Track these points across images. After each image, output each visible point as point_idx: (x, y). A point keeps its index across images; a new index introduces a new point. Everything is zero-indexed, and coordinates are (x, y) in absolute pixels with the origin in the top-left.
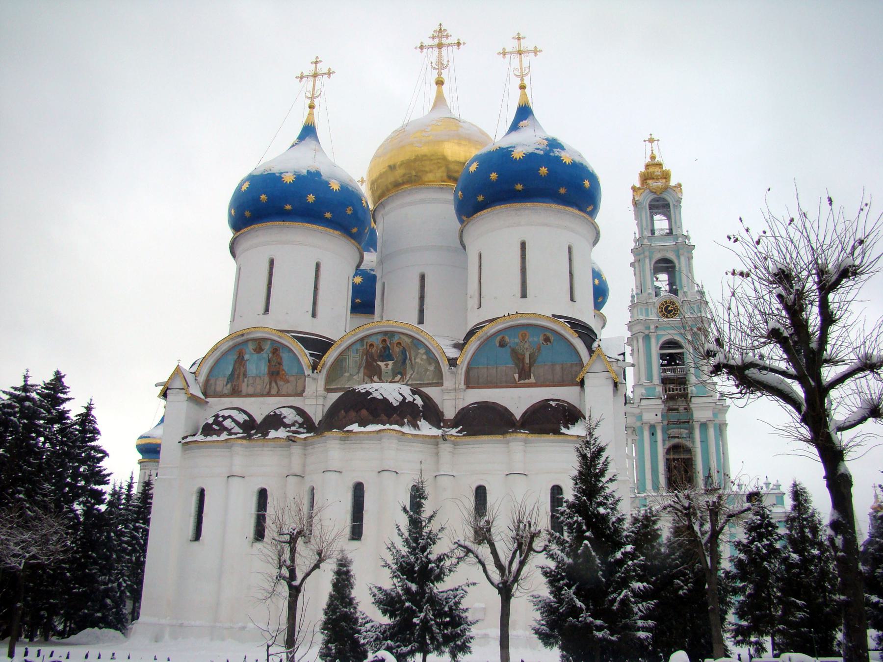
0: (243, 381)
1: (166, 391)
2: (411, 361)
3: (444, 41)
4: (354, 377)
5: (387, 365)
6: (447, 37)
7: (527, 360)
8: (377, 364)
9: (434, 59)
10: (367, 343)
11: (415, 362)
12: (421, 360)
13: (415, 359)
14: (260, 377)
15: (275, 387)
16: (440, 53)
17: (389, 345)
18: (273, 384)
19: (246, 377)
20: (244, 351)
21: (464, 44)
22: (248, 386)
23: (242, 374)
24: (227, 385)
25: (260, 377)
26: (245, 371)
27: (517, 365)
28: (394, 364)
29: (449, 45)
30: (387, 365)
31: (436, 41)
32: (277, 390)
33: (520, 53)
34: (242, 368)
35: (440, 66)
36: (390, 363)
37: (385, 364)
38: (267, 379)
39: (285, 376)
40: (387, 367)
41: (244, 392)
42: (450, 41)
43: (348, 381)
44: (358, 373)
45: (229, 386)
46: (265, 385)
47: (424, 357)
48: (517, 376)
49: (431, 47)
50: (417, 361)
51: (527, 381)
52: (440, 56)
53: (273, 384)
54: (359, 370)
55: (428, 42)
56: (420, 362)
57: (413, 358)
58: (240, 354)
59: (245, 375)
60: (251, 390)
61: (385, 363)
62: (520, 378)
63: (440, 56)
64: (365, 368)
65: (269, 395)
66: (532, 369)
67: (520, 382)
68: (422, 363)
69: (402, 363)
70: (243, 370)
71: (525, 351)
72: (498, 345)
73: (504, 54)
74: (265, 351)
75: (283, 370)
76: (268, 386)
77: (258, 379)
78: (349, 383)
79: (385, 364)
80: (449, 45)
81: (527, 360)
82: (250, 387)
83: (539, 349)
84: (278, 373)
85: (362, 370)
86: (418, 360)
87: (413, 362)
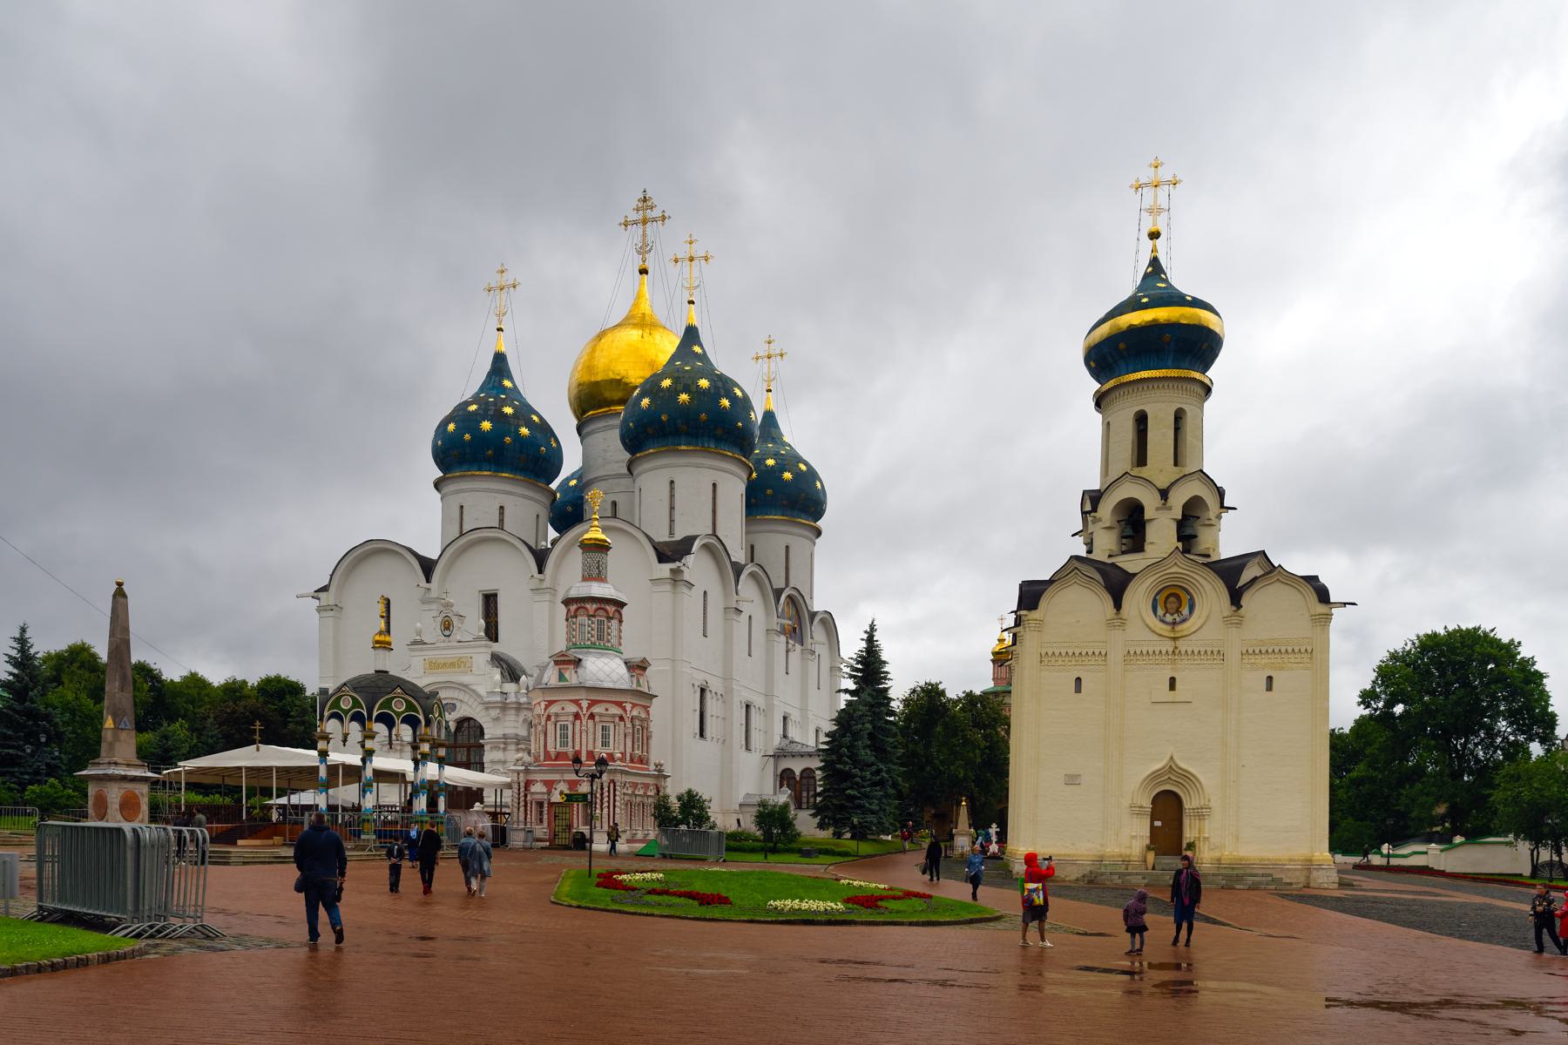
3: (650, 214)
6: (652, 208)
9: (638, 240)
16: (644, 231)
21: (670, 217)
29: (654, 220)
31: (639, 216)
33: (691, 259)
35: (644, 250)
42: (656, 213)
49: (635, 223)
52: (644, 235)
55: (633, 216)
63: (644, 235)
73: (676, 261)
80: (654, 220)
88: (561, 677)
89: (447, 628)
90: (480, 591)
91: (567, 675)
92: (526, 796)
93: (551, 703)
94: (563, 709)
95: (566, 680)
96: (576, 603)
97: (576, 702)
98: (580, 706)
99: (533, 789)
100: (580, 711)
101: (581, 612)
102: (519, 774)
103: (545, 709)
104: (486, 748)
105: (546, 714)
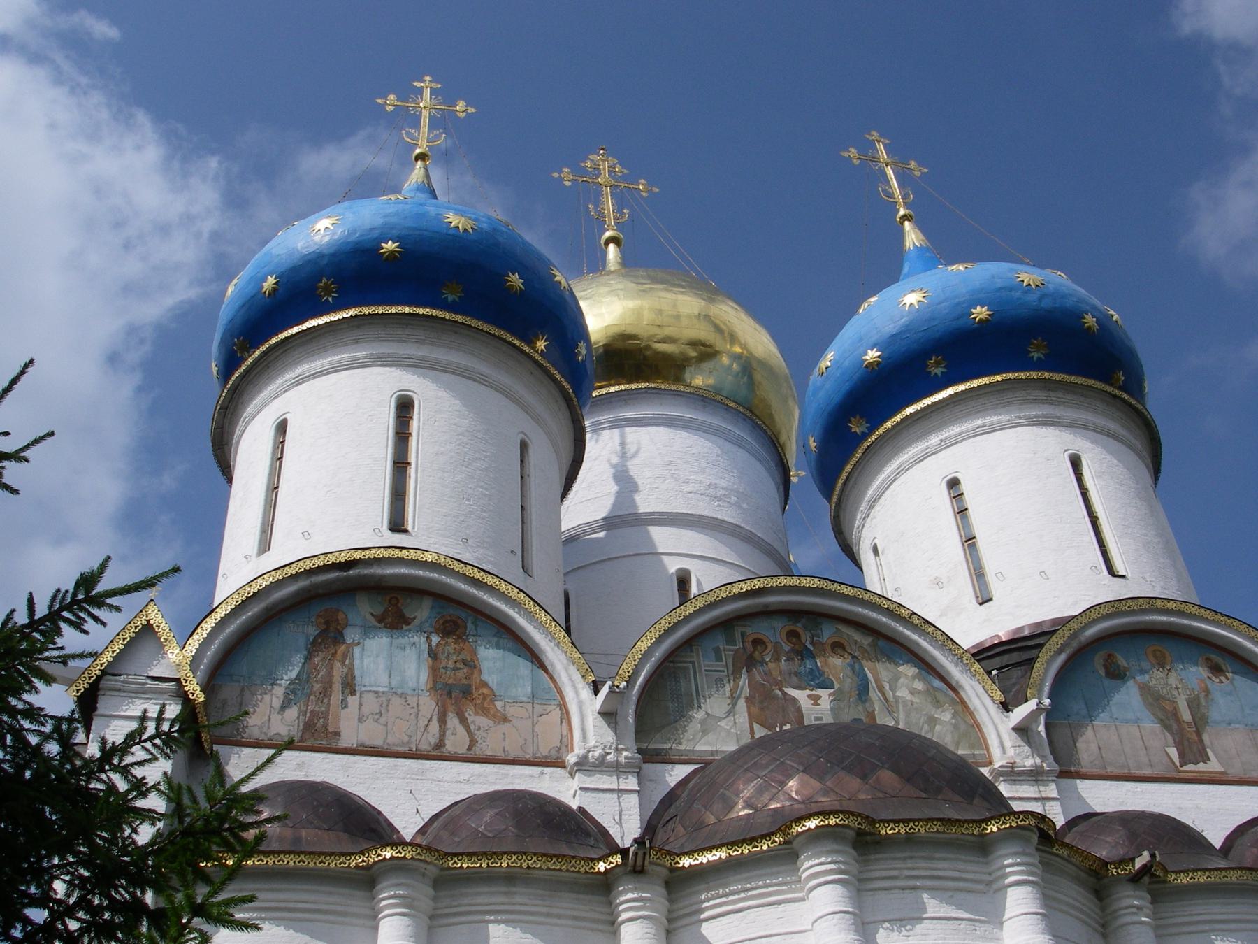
0: (344, 704)
1: (99, 678)
2: (884, 694)
4: (722, 723)
5: (816, 699)
7: (1186, 716)
8: (785, 694)
10: (743, 634)
11: (897, 699)
12: (912, 693)
13: (893, 689)
14: (403, 696)
15: (461, 730)
17: (811, 648)
18: (453, 721)
19: (353, 692)
20: (341, 616)
22: (360, 720)
23: (337, 686)
24: (283, 708)
25: (403, 696)
26: (351, 669)
27: (1167, 727)
28: (837, 698)
30: (816, 699)
32: (467, 740)
34: (337, 665)
36: (824, 694)
37: (809, 696)
38: (428, 705)
39: (492, 701)
40: (816, 704)
41: (346, 741)
43: (705, 732)
44: (731, 712)
45: (292, 713)
46: (423, 722)
47: (919, 685)
48: (1173, 752)
50: (897, 694)
51: (1201, 767)
53: (453, 721)
54: (734, 704)
56: (909, 697)
57: (887, 686)
58: (327, 623)
59: (349, 686)
60: (371, 734)
61: (808, 692)
62: (1184, 760)
64: (749, 700)
65: (437, 754)
66: (1206, 737)
67: (1185, 768)
68: (916, 700)
69: (859, 695)
70: (339, 671)
71: (1175, 693)
72: (1104, 675)
74: (417, 622)
75: (485, 684)
76: (435, 727)
77: (396, 701)
78: (711, 737)
79: (809, 696)
81: (1186, 716)
82: (370, 721)
83: (1207, 692)
84: (467, 692)
85: (742, 703)
86: (903, 693)
87: (891, 698)
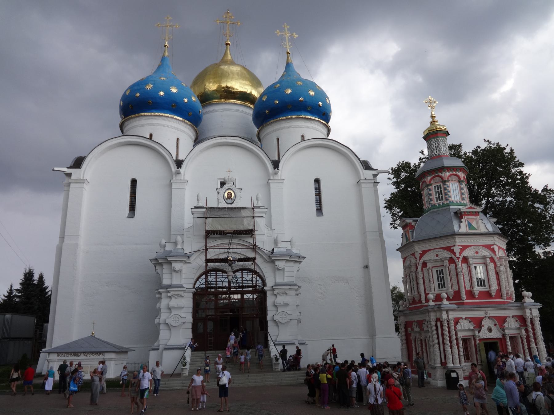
88: (470, 226)
89: (229, 197)
90: (219, 179)
91: (474, 224)
92: (456, 334)
93: (465, 247)
94: (477, 253)
95: (474, 228)
96: (448, 171)
97: (489, 247)
98: (493, 250)
99: (459, 327)
100: (493, 255)
101: (453, 176)
102: (447, 312)
103: (460, 253)
104: (268, 294)
105: (461, 257)
